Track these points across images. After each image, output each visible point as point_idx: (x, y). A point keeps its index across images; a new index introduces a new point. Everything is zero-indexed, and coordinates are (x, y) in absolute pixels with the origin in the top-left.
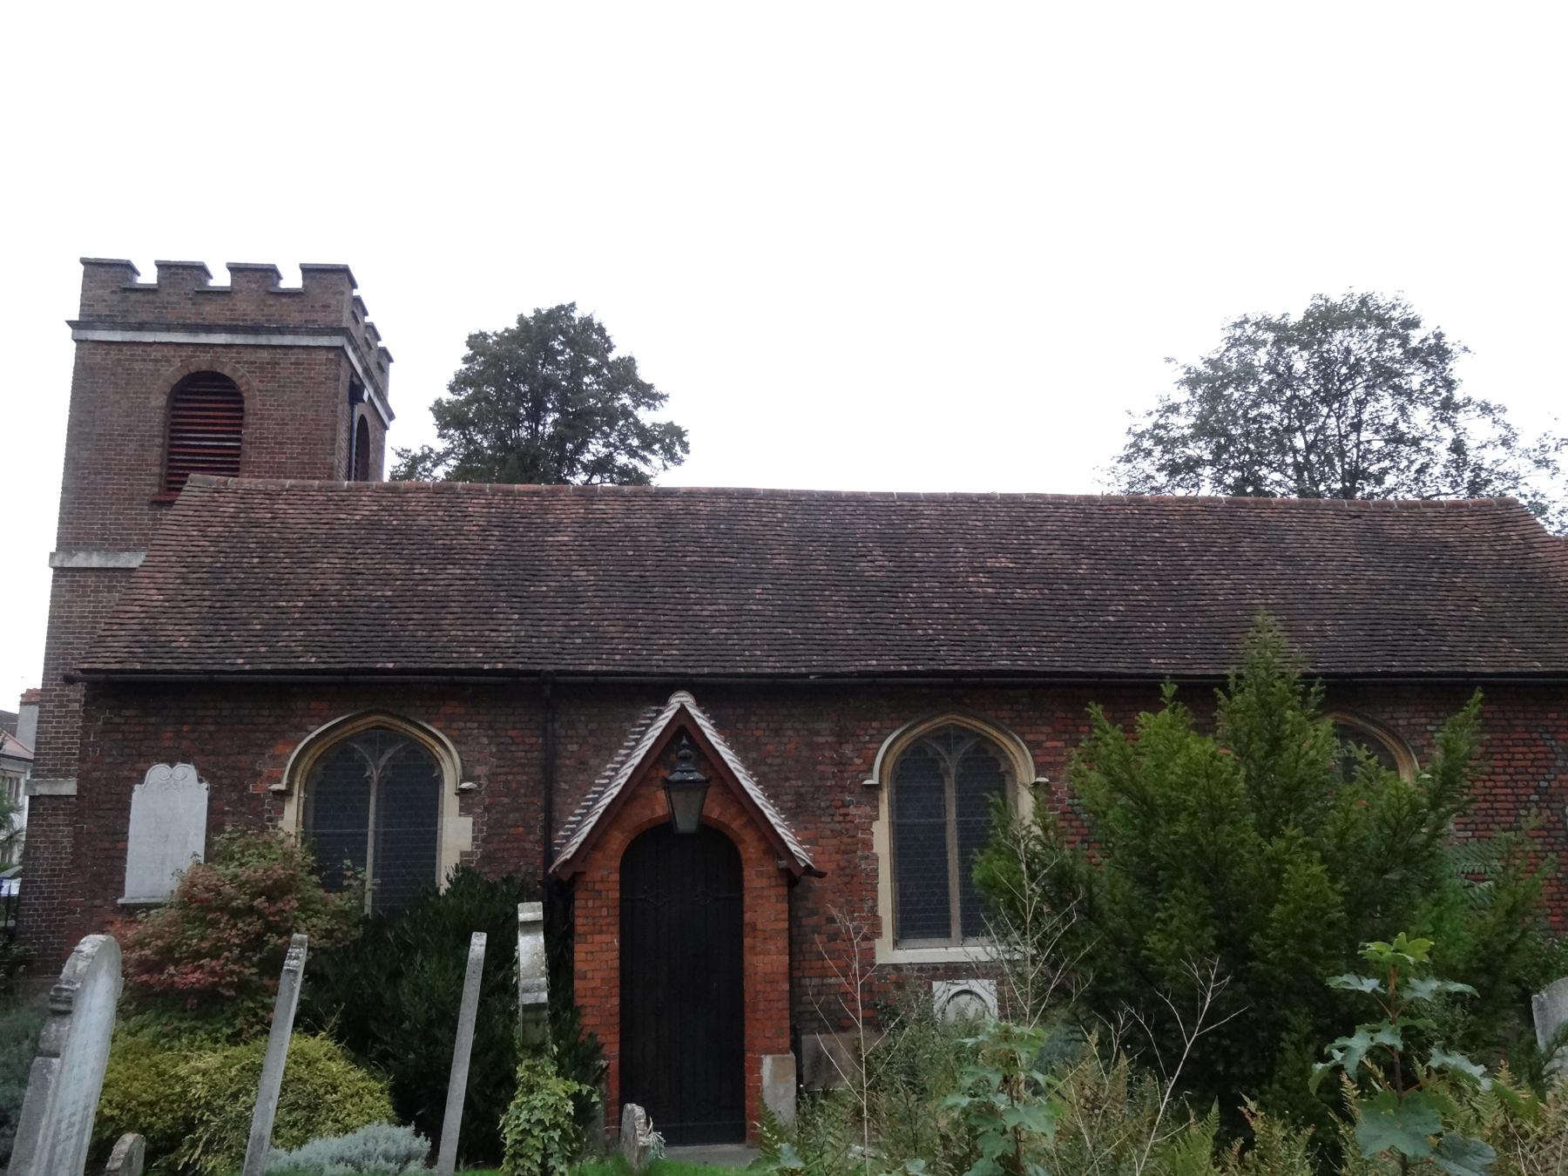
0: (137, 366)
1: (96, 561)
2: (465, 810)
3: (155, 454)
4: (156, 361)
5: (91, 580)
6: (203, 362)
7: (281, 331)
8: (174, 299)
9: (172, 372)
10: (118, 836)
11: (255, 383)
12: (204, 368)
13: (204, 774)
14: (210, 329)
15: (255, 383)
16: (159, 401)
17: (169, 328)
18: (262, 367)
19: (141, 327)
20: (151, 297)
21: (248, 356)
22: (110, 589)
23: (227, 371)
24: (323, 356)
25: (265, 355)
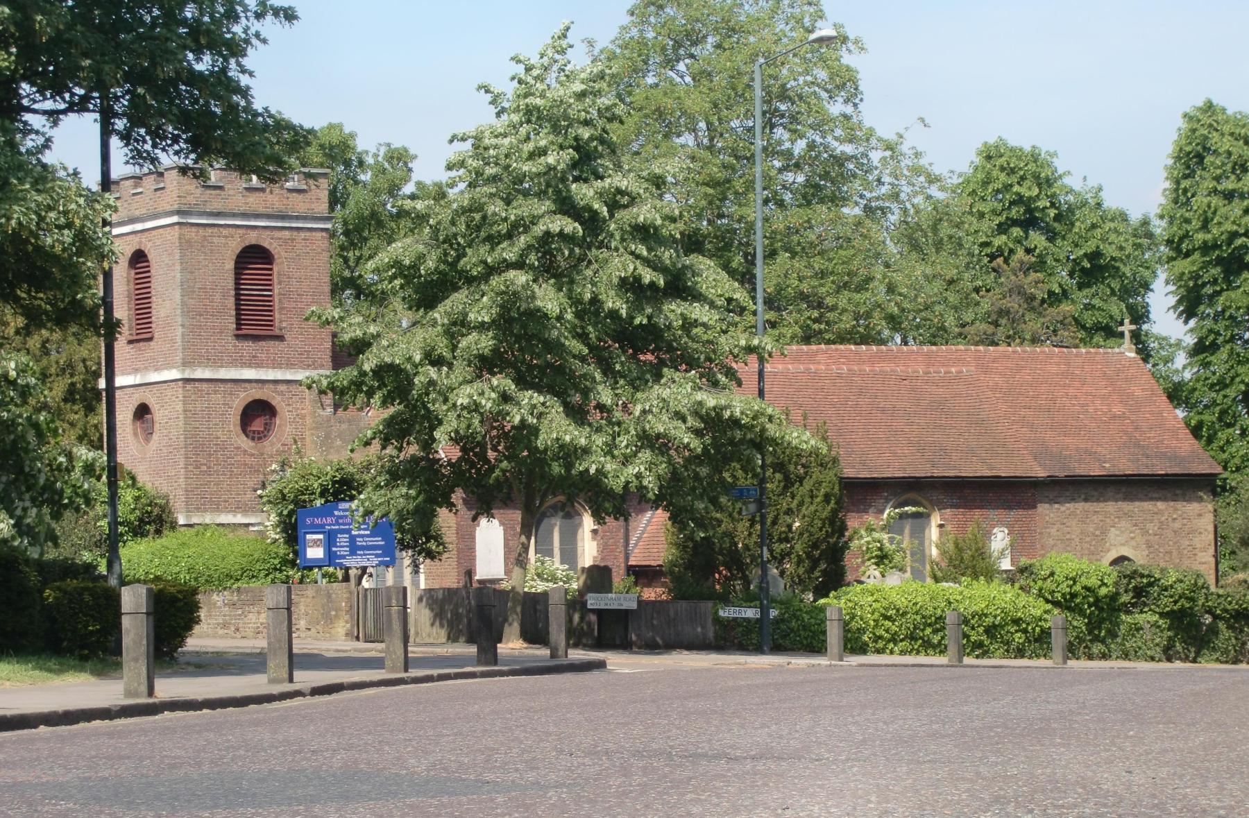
0: (215, 240)
1: (207, 374)
2: (594, 539)
3: (231, 302)
4: (226, 237)
5: (205, 386)
6: (252, 238)
7: (297, 218)
8: (231, 192)
9: (235, 245)
10: (472, 549)
11: (283, 254)
12: (254, 242)
13: (501, 523)
14: (258, 216)
15: (283, 254)
16: (230, 265)
17: (234, 215)
18: (286, 241)
19: (218, 215)
20: (218, 192)
21: (277, 234)
22: (215, 392)
23: (266, 245)
24: (319, 234)
25: (287, 234)
